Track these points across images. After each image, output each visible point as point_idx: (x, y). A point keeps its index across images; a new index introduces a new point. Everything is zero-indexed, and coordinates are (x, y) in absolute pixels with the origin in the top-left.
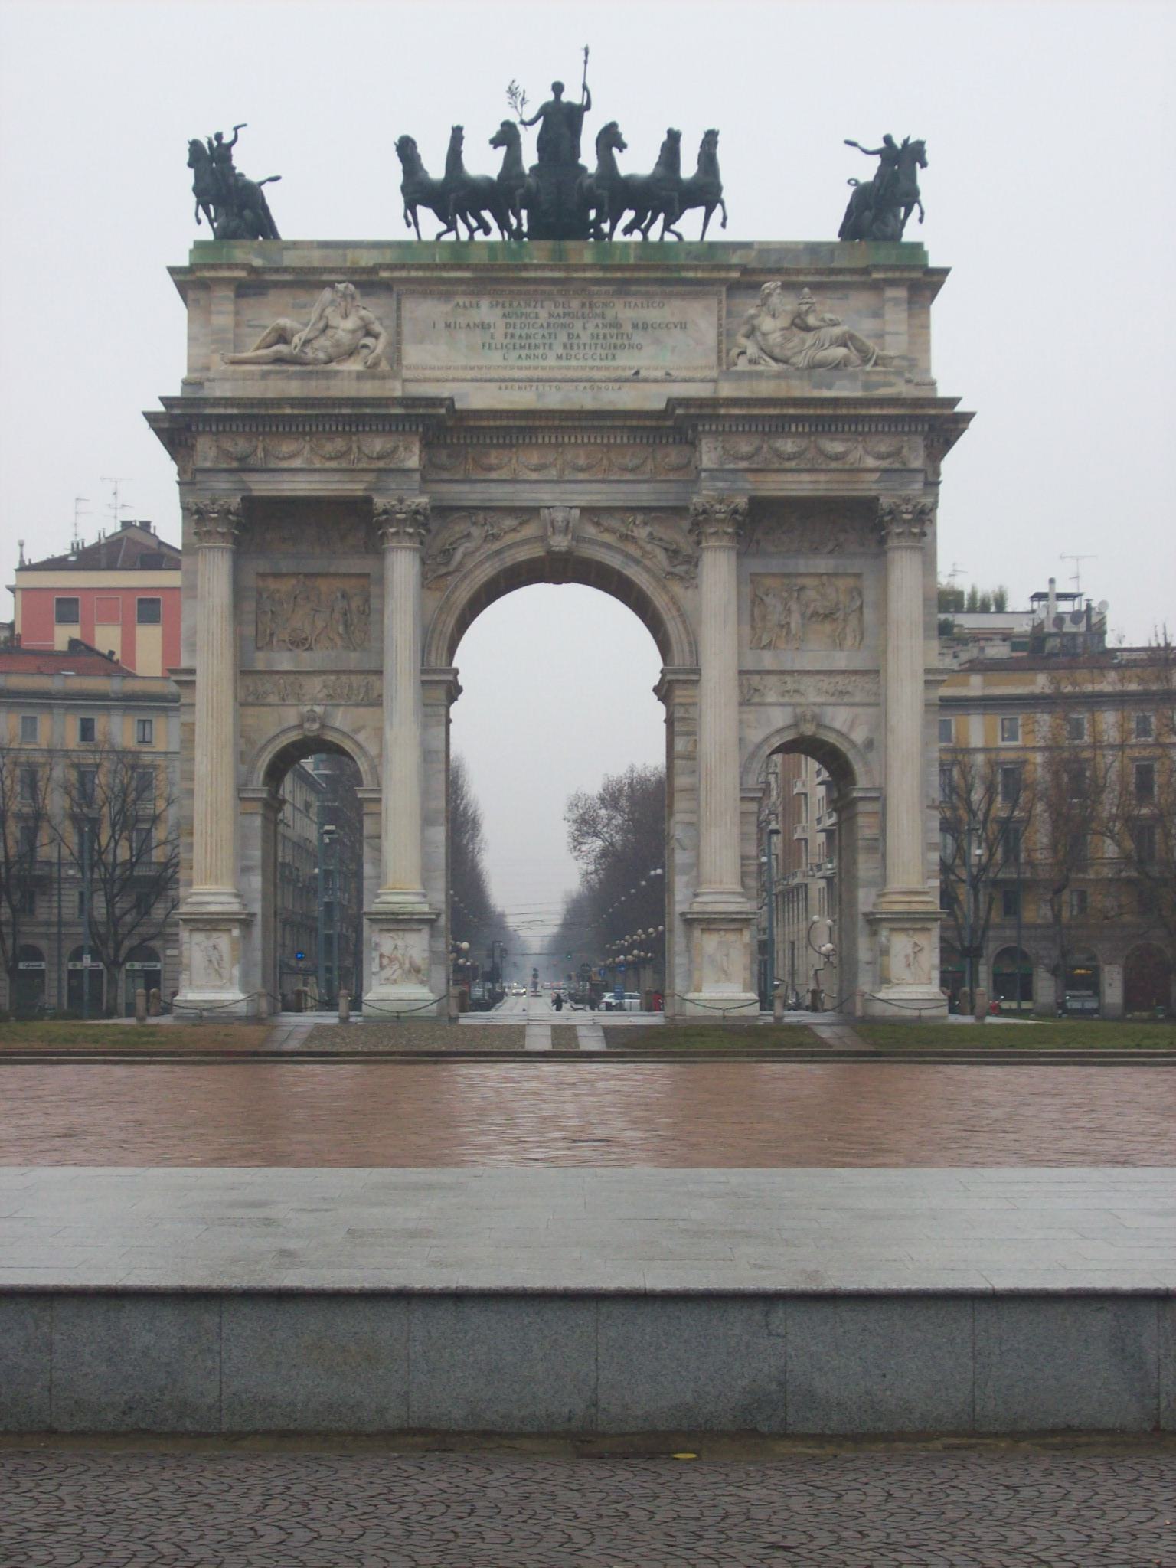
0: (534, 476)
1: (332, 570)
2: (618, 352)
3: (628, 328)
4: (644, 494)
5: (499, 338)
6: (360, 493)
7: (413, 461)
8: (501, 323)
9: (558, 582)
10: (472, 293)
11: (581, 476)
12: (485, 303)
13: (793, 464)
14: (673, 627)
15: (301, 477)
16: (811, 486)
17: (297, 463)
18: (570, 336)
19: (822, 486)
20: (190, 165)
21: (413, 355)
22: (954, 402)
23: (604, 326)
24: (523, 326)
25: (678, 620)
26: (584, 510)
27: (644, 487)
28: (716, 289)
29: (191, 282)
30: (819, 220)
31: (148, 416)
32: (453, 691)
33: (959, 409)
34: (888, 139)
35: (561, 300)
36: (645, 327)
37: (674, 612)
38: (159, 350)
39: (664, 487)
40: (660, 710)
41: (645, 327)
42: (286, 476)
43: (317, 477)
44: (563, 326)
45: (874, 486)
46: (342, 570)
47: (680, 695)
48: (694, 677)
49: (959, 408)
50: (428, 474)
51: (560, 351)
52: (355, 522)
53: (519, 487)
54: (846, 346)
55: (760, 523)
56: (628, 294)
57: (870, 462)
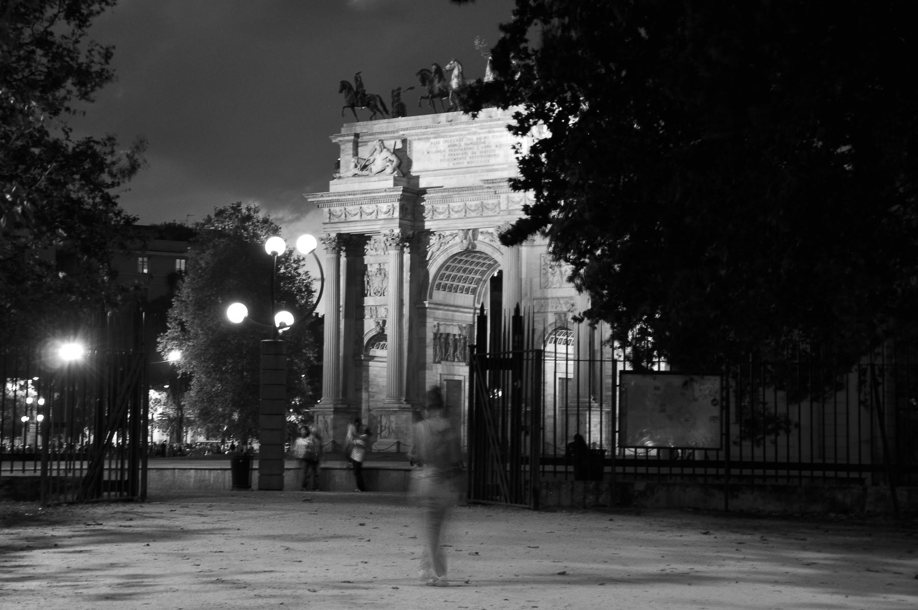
3: (493, 147)
5: (447, 157)
8: (447, 150)
11: (473, 214)
12: (441, 140)
15: (358, 224)
18: (473, 153)
20: (341, 91)
24: (455, 150)
43: (364, 223)
51: (468, 159)
53: (450, 221)
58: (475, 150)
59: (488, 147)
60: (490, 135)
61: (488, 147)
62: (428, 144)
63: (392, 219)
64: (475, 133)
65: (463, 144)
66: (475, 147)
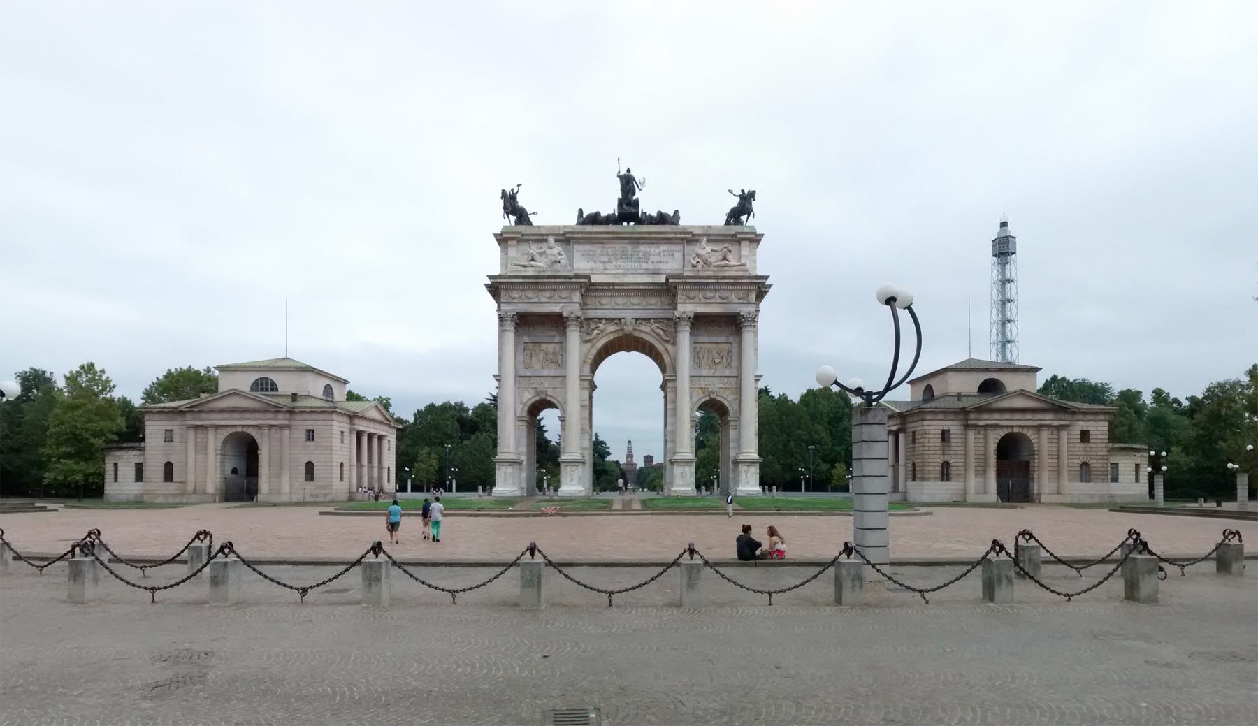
4: (660, 314)
9: (629, 350)
14: (667, 360)
21: (576, 266)
22: (766, 278)
26: (637, 319)
29: (503, 239)
30: (717, 219)
31: (487, 286)
32: (593, 387)
33: (768, 282)
38: (492, 262)
40: (662, 394)
47: (669, 385)
49: (768, 282)
50: (584, 305)
52: (557, 322)
55: (700, 322)
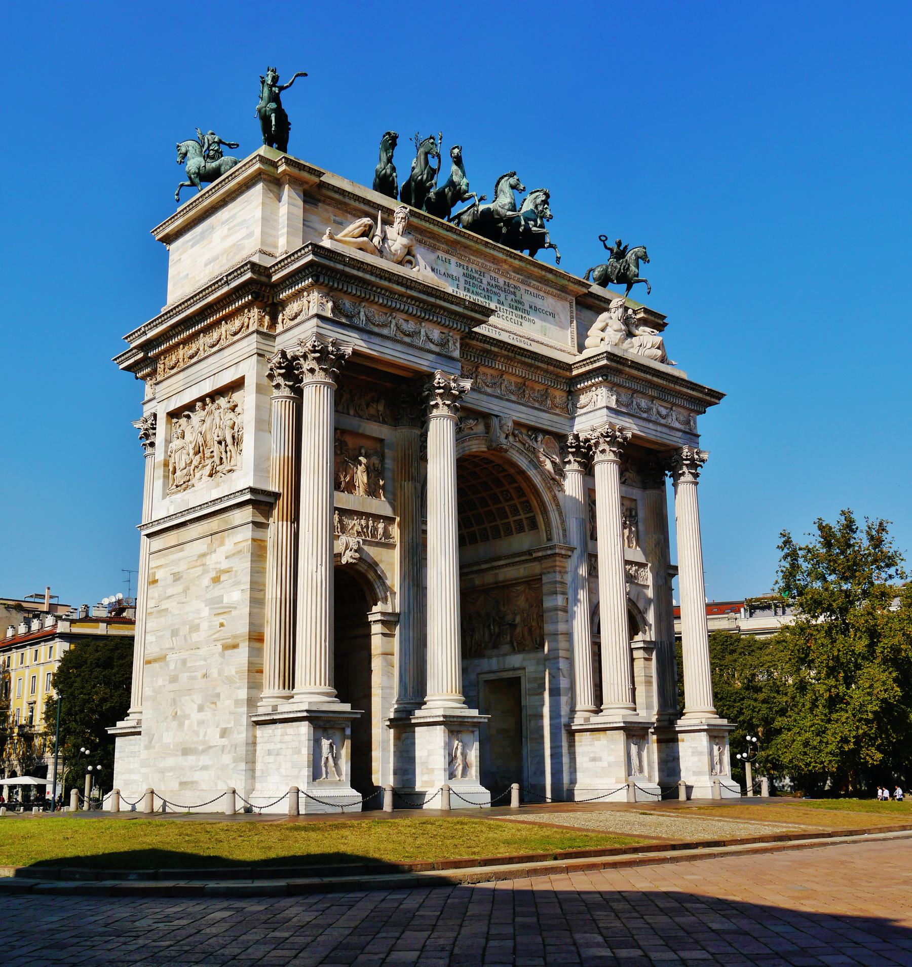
0: (489, 390)
1: (361, 431)
2: (523, 321)
3: (527, 307)
6: (425, 369)
7: (456, 354)
8: (462, 279)
10: (447, 252)
11: (513, 398)
12: (454, 260)
13: (645, 415)
15: (388, 344)
16: (654, 433)
17: (385, 332)
19: (658, 434)
23: (516, 301)
24: (474, 285)
25: (556, 513)
27: (545, 416)
28: (570, 298)
34: (619, 244)
35: (493, 274)
36: (536, 309)
37: (555, 508)
39: (555, 418)
41: (536, 309)
42: (377, 340)
43: (399, 347)
44: (495, 294)
45: (680, 441)
46: (368, 433)
48: (570, 553)
54: (658, 348)
56: (529, 285)
57: (677, 425)
58: (502, 299)
59: (520, 302)
60: (523, 287)
61: (520, 302)
62: (433, 257)
63: (452, 359)
64: (505, 274)
65: (485, 281)
66: (503, 295)
